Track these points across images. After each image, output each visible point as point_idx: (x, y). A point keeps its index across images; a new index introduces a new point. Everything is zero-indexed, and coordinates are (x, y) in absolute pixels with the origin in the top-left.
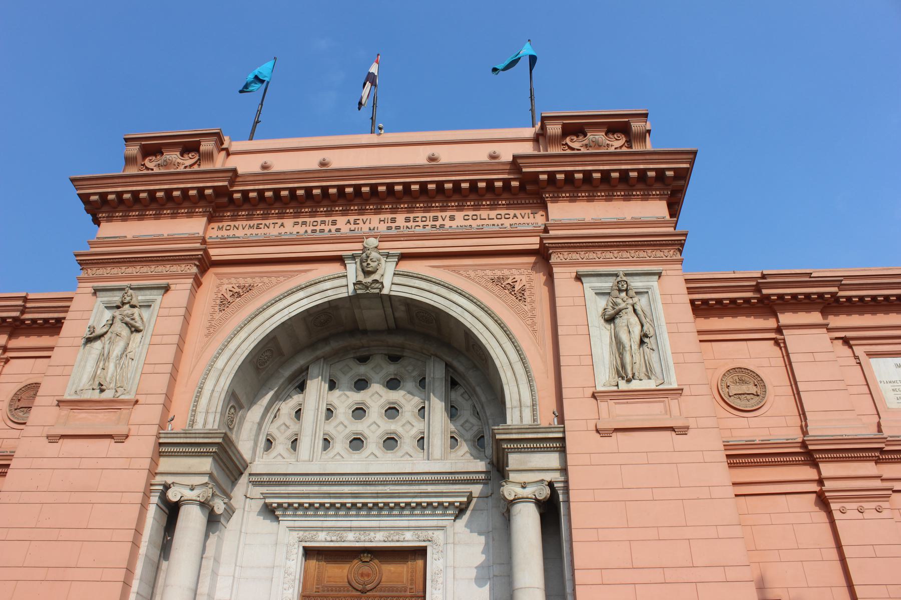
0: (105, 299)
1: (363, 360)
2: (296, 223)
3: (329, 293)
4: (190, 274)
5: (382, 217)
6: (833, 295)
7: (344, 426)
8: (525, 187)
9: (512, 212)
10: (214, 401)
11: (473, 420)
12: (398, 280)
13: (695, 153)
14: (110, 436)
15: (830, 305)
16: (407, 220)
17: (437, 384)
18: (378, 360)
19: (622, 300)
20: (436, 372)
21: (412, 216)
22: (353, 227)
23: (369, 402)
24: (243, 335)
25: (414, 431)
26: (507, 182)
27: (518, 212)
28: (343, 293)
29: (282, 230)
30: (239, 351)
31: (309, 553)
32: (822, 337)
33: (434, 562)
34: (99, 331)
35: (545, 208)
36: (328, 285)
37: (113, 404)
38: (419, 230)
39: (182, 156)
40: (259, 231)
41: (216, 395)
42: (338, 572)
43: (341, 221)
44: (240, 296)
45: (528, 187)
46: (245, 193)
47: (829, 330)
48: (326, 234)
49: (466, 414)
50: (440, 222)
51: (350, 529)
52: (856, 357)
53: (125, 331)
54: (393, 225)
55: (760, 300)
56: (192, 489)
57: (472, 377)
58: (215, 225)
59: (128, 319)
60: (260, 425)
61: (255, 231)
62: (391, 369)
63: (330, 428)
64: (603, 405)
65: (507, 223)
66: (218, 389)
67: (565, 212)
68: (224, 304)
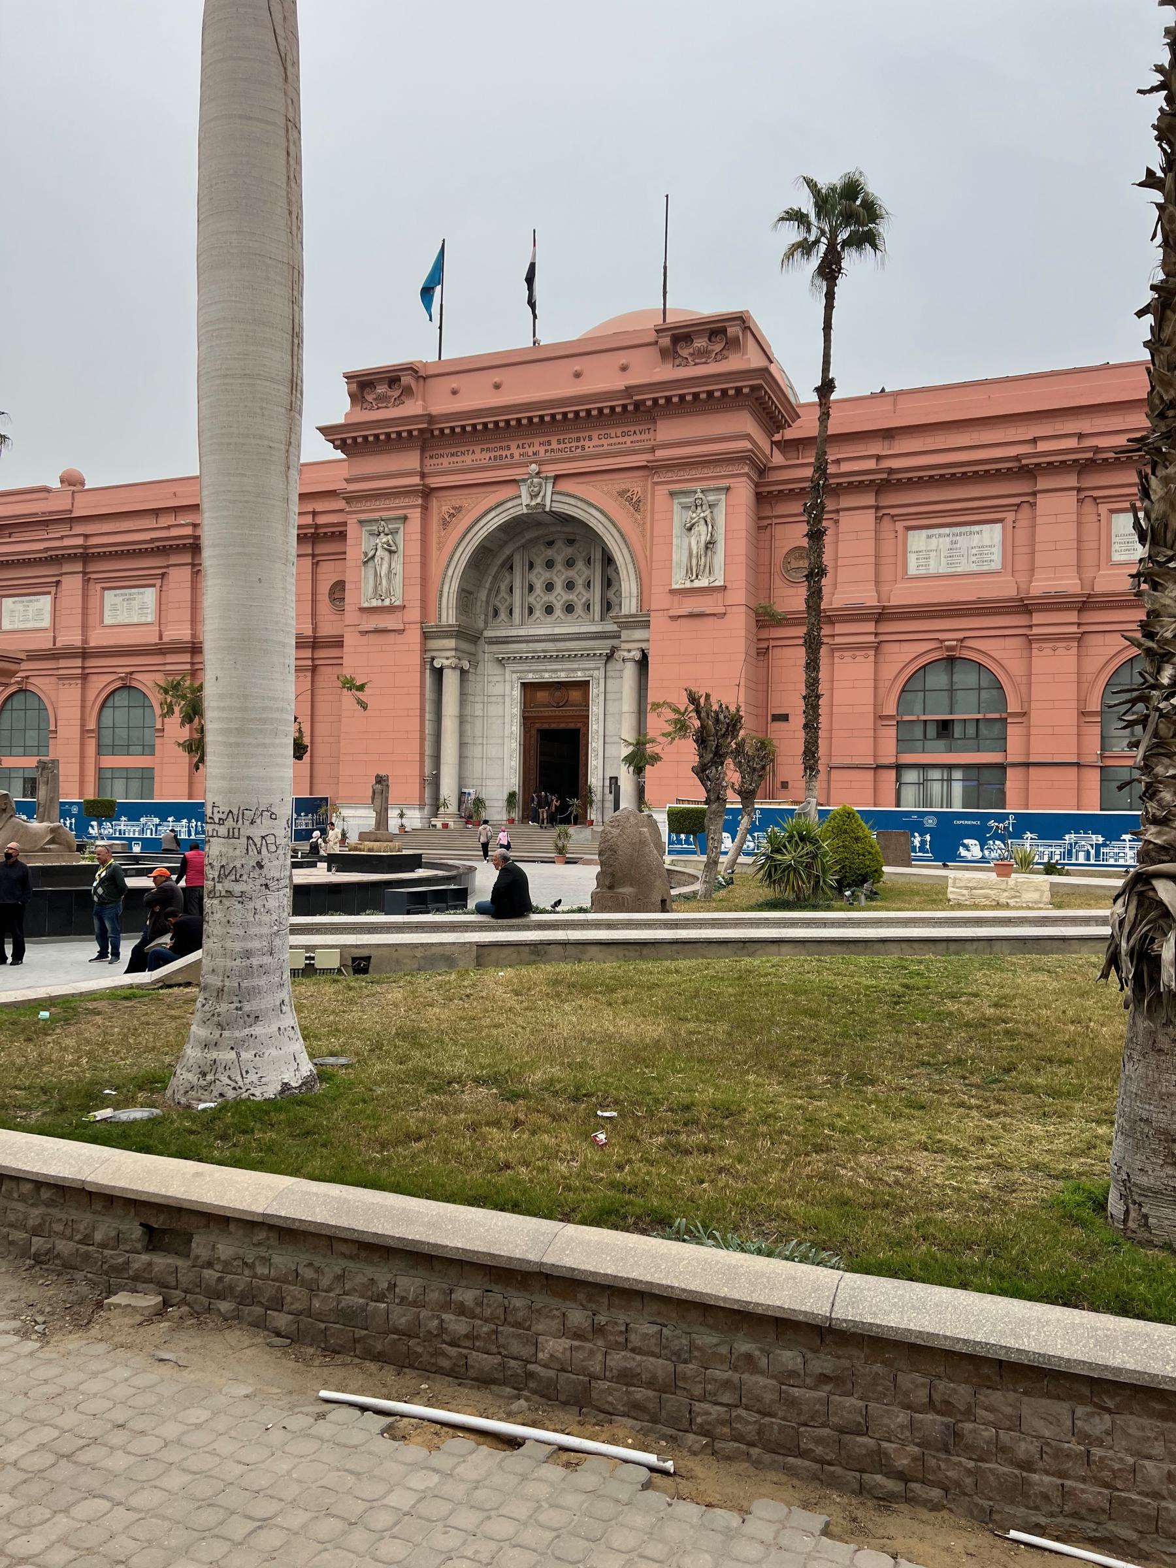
1: (550, 544)
2: (482, 450)
3: (512, 511)
5: (542, 440)
7: (539, 598)
8: (638, 409)
9: (632, 429)
12: (556, 497)
16: (559, 442)
18: (559, 544)
21: (561, 437)
23: (555, 578)
24: (461, 549)
27: (637, 428)
29: (474, 457)
31: (524, 685)
32: (870, 515)
33: (594, 691)
34: (371, 554)
36: (510, 504)
37: (392, 609)
42: (542, 696)
43: (513, 445)
45: (642, 409)
46: (442, 430)
50: (579, 444)
54: (549, 448)
56: (447, 658)
60: (487, 602)
61: (455, 459)
62: (568, 551)
63: (531, 599)
65: (628, 439)
67: (668, 430)
68: (445, 524)
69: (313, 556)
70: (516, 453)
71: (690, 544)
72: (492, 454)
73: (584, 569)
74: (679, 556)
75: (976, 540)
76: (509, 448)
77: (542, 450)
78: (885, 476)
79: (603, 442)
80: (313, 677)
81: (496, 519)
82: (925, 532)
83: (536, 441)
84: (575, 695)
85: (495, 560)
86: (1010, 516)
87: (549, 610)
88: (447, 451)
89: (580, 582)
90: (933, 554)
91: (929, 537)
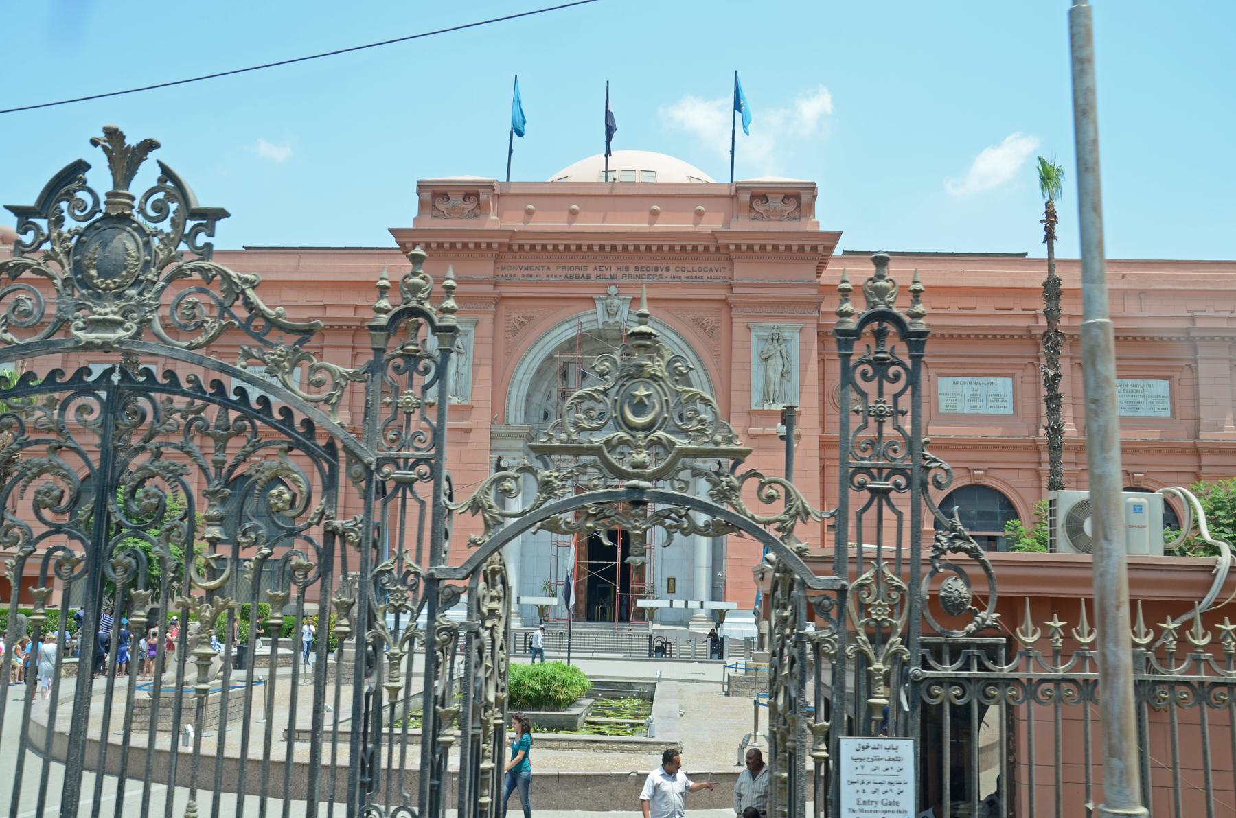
2: (558, 267)
8: (721, 251)
13: (840, 234)
16: (637, 269)
19: (775, 349)
22: (599, 273)
24: (531, 356)
26: (707, 248)
28: (594, 326)
44: (524, 324)
46: (521, 247)
58: (499, 265)
64: (754, 418)
65: (705, 275)
67: (743, 271)
68: (514, 331)
69: (353, 348)
70: (593, 274)
71: (766, 371)
72: (569, 273)
74: (757, 382)
75: (992, 389)
77: (620, 273)
79: (680, 274)
82: (951, 379)
83: (614, 267)
85: (558, 369)
86: (1019, 373)
90: (959, 398)
91: (955, 383)
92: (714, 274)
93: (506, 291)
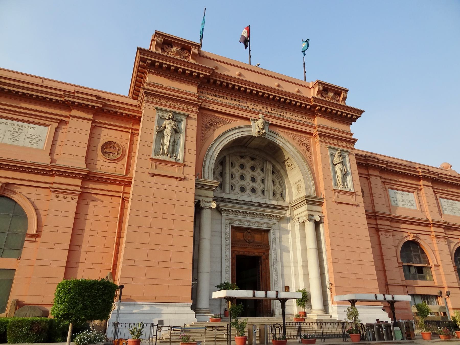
0: (160, 114)
1: (242, 157)
2: (232, 99)
3: (246, 133)
4: (197, 112)
6: (385, 167)
10: (210, 168)
11: (280, 187)
14: (176, 178)
15: (382, 170)
17: (269, 172)
18: (248, 158)
20: (270, 167)
22: (253, 107)
25: (261, 188)
30: (217, 150)
35: (315, 118)
36: (245, 129)
38: (275, 115)
39: (181, 49)
40: (218, 99)
41: (210, 166)
42: (239, 235)
46: (215, 81)
47: (381, 178)
48: (243, 108)
49: (277, 185)
50: (282, 114)
51: (246, 221)
52: (386, 188)
53: (174, 132)
55: (366, 164)
56: (208, 202)
57: (282, 172)
59: (174, 127)
61: (216, 98)
62: (252, 163)
63: (233, 181)
65: (303, 120)
66: (211, 164)
68: (207, 127)
69: (93, 122)
70: (251, 107)
72: (238, 103)
73: (261, 173)
76: (246, 103)
77: (264, 110)
78: (385, 166)
80: (79, 199)
81: (238, 134)
84: (258, 237)
87: (242, 189)
88: (212, 93)
89: (259, 179)
92: (307, 120)
93: (205, 105)
